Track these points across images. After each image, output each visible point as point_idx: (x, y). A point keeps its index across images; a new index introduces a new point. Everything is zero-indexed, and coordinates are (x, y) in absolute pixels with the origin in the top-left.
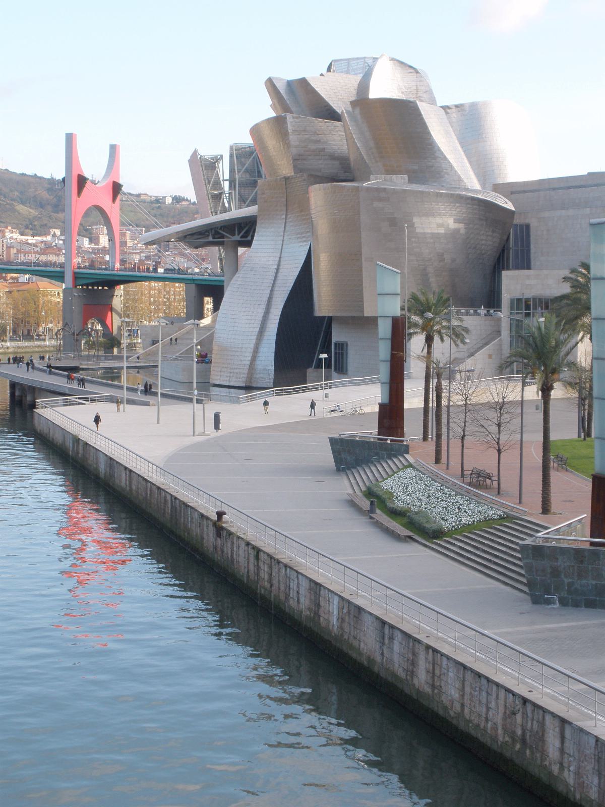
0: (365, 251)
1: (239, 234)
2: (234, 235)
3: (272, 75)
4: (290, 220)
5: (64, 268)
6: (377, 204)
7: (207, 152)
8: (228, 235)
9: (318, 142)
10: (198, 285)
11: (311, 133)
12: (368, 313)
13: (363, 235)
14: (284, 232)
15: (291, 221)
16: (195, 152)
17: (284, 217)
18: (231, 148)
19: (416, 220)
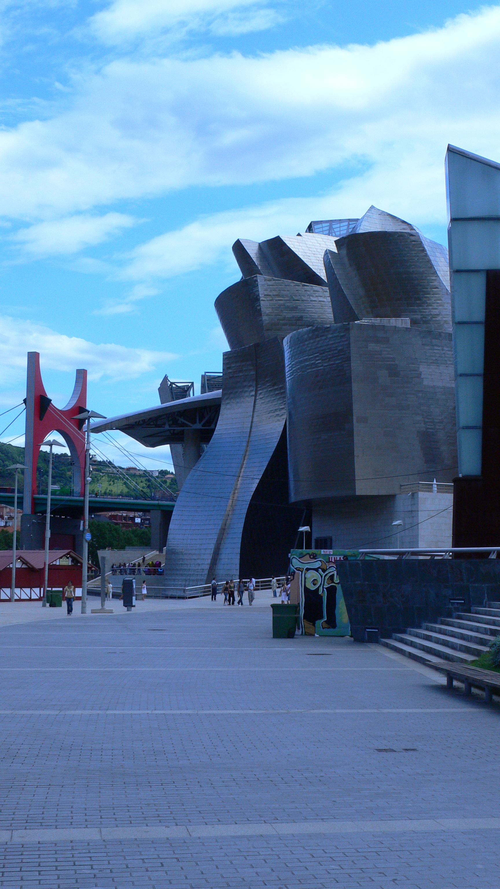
0: (357, 409)
1: (200, 421)
2: (194, 422)
3: (242, 237)
4: (261, 396)
5: (22, 493)
6: (372, 346)
7: (178, 379)
8: (189, 424)
9: (295, 308)
10: (163, 511)
11: (286, 299)
12: (362, 488)
13: (355, 387)
14: (253, 412)
15: (261, 398)
16: (166, 378)
17: (253, 393)
18: (203, 377)
19: (423, 369)
